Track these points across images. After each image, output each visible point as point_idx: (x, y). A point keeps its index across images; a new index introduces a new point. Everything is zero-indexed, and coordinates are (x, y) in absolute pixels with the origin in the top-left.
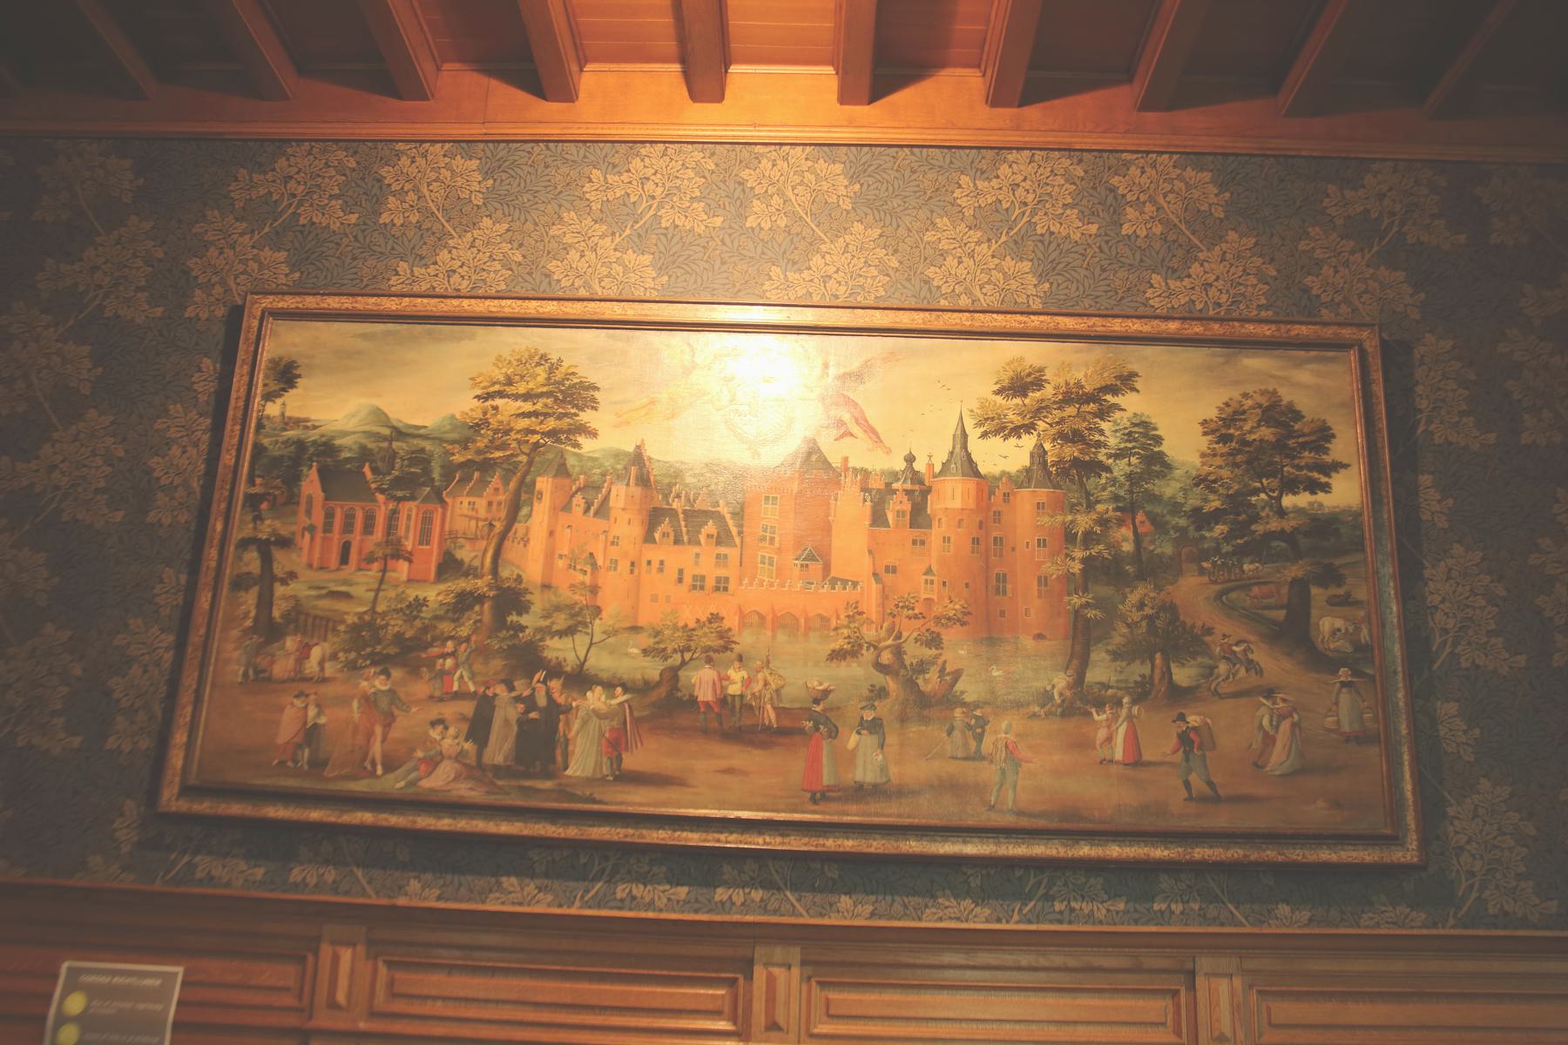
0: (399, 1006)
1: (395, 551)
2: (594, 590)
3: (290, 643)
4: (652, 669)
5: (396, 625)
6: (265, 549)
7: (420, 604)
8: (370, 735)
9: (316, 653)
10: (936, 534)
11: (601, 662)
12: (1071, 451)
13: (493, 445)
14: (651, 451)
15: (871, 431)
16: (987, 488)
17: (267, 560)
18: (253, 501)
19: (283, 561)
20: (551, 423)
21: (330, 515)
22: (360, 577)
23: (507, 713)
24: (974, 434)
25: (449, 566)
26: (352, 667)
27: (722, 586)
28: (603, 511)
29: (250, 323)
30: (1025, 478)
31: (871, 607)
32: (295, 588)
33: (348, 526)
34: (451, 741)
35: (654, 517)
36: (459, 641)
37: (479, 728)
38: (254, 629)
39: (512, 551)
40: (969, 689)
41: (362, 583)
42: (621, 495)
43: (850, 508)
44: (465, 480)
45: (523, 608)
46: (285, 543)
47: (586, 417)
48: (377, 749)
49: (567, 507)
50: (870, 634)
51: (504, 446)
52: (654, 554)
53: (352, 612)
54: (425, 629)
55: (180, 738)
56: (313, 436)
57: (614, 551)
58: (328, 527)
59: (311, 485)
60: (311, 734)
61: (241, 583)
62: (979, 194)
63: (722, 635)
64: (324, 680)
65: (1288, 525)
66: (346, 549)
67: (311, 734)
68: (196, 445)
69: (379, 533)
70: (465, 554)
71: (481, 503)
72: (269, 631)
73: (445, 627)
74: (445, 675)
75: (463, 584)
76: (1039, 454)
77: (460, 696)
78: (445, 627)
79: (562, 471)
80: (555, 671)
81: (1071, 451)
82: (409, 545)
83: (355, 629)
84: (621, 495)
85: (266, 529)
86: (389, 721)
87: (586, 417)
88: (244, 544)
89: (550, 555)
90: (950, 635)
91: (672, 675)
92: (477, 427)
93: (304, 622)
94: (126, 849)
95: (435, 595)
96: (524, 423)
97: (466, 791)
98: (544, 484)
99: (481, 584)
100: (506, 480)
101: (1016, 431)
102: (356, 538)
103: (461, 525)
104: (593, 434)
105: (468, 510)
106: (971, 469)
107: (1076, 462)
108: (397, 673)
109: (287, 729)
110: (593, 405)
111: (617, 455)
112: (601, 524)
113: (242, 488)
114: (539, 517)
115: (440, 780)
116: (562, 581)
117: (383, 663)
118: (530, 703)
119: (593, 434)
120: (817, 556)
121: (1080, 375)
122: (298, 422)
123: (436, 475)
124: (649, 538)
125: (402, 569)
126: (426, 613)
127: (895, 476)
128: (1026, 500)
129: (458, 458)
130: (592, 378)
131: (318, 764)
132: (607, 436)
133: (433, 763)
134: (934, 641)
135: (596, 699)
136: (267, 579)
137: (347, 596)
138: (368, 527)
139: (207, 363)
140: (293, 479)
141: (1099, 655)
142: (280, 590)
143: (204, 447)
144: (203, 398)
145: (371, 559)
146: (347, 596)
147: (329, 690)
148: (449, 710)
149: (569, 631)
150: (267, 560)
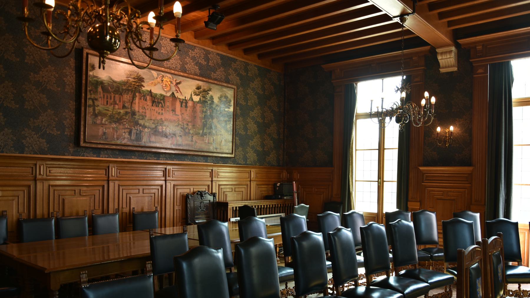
0: (121, 176)
1: (115, 103)
2: (145, 113)
3: (99, 118)
4: (153, 126)
5: (117, 116)
6: (93, 100)
7: (120, 113)
8: (114, 134)
9: (104, 120)
10: (188, 109)
11: (147, 124)
12: (204, 99)
13: (128, 87)
14: (152, 91)
15: (181, 92)
16: (194, 102)
17: (94, 103)
18: (90, 91)
19: (96, 103)
20: (138, 84)
21: (104, 96)
22: (110, 107)
23: (134, 131)
24: (193, 95)
25: (124, 107)
26: (110, 122)
27: (162, 114)
28: (146, 100)
29: (85, 55)
30: (198, 102)
31: (180, 119)
32: (98, 108)
33: (107, 98)
34: (127, 135)
35: (153, 102)
36: (126, 119)
37: (130, 133)
38: (92, 115)
39: (133, 105)
40: (191, 132)
41: (111, 108)
42: (148, 98)
43: (178, 104)
44: (125, 92)
45: (135, 115)
46: (96, 100)
47: (143, 83)
48: (115, 136)
49: (141, 99)
50: (180, 123)
51: (131, 87)
52: (153, 108)
53: (109, 113)
54: (121, 117)
55: (82, 133)
56: (100, 80)
57: (148, 107)
58: (104, 98)
59: (100, 89)
60: (104, 133)
61: (90, 106)
62: (192, 54)
63: (163, 121)
64: (106, 125)
65: (226, 113)
66: (107, 102)
67: (104, 133)
68: (73, 76)
69: (112, 100)
70: (126, 105)
71: (128, 97)
72: (96, 115)
73: (124, 117)
74: (124, 125)
75: (126, 110)
76: (200, 99)
77: (127, 128)
78: (124, 117)
79: (140, 92)
80: (140, 125)
81: (204, 99)
82: (117, 102)
83: (110, 116)
84: (148, 98)
85: (93, 96)
86: (117, 132)
87: (143, 83)
88: (90, 99)
89: (139, 106)
90: (190, 124)
91: (156, 127)
92: (127, 82)
93: (100, 114)
94: (72, 152)
95: (122, 111)
96: (133, 83)
97: (129, 143)
98: (137, 94)
99: (129, 110)
100: (132, 93)
101: (198, 95)
102: (109, 100)
103: (125, 100)
104: (144, 87)
105: (126, 97)
106: (192, 100)
107: (204, 101)
108: (117, 124)
109: (100, 133)
110: (143, 82)
111: (148, 91)
112: (146, 102)
113: (88, 88)
114: (137, 100)
115: (125, 142)
116: (141, 111)
117: (115, 122)
118: (137, 130)
119: (144, 87)
120: (174, 110)
121: (205, 88)
122: (96, 77)
123: (121, 90)
124: (152, 105)
125: (117, 107)
126: (121, 114)
127: (183, 100)
128: (199, 105)
129: (124, 88)
130: (144, 77)
131: (106, 139)
132: (146, 87)
133: (124, 138)
134: (188, 125)
135: (146, 130)
136: (94, 106)
137: (108, 110)
138: (111, 98)
139: (72, 59)
140: (96, 88)
141: (205, 128)
142: (96, 108)
143: (74, 77)
144: (72, 67)
145: (111, 104)
146: (108, 110)
147: (107, 126)
148: (126, 131)
149: (142, 119)
150: (94, 103)
